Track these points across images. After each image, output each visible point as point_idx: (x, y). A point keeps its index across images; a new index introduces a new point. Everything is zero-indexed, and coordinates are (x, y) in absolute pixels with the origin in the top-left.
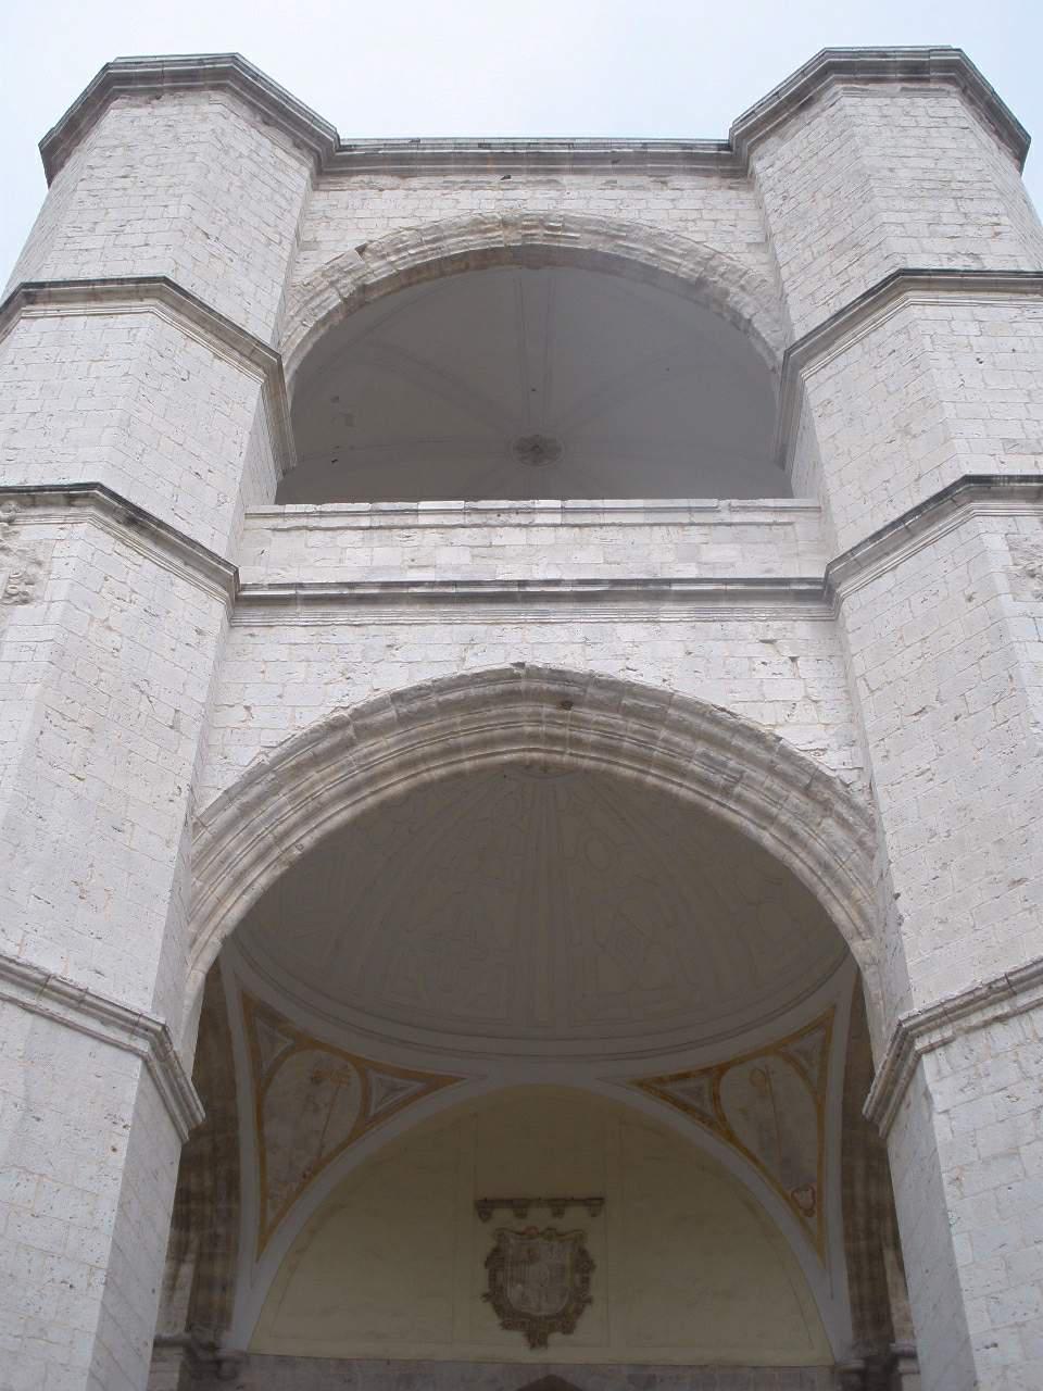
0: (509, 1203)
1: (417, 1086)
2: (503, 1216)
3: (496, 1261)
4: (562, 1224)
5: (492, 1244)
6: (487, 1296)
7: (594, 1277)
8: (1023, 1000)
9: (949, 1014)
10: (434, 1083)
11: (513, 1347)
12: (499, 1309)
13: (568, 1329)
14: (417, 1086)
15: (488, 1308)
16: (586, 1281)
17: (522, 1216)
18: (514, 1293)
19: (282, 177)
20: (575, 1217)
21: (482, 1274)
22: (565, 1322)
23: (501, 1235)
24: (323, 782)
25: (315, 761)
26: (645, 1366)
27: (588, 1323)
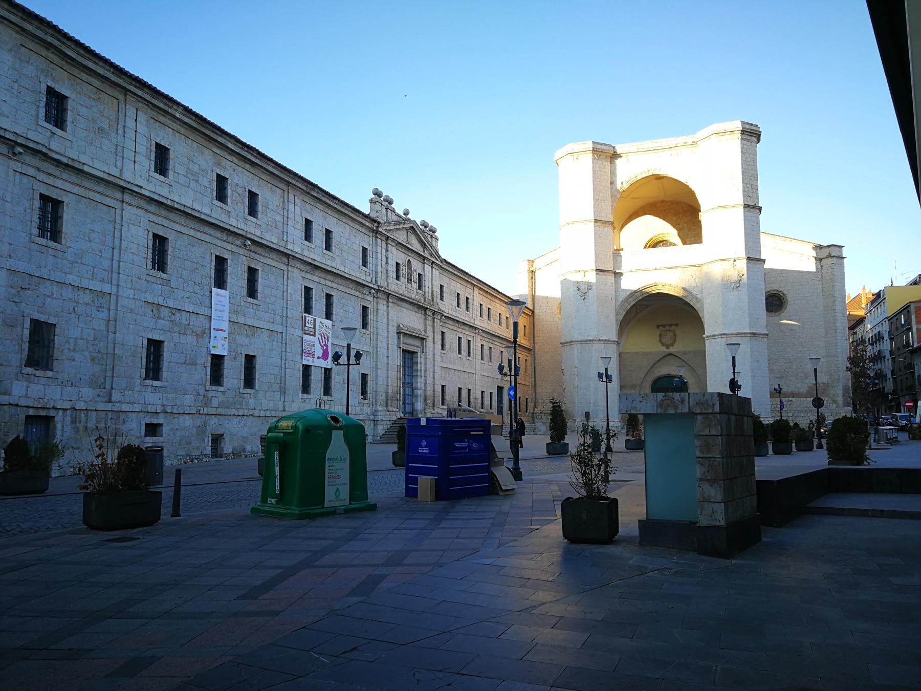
0: (662, 326)
1: (645, 307)
2: (661, 328)
3: (660, 335)
4: (670, 328)
5: (659, 333)
6: (659, 341)
7: (677, 337)
8: (715, 337)
9: (708, 337)
10: (648, 306)
11: (664, 349)
12: (661, 343)
13: (673, 346)
14: (645, 307)
15: (659, 343)
16: (676, 338)
17: (664, 328)
18: (664, 341)
19: (605, 170)
20: (673, 328)
21: (658, 338)
22: (672, 345)
23: (661, 331)
24: (631, 300)
25: (630, 298)
26: (685, 351)
27: (675, 345)
